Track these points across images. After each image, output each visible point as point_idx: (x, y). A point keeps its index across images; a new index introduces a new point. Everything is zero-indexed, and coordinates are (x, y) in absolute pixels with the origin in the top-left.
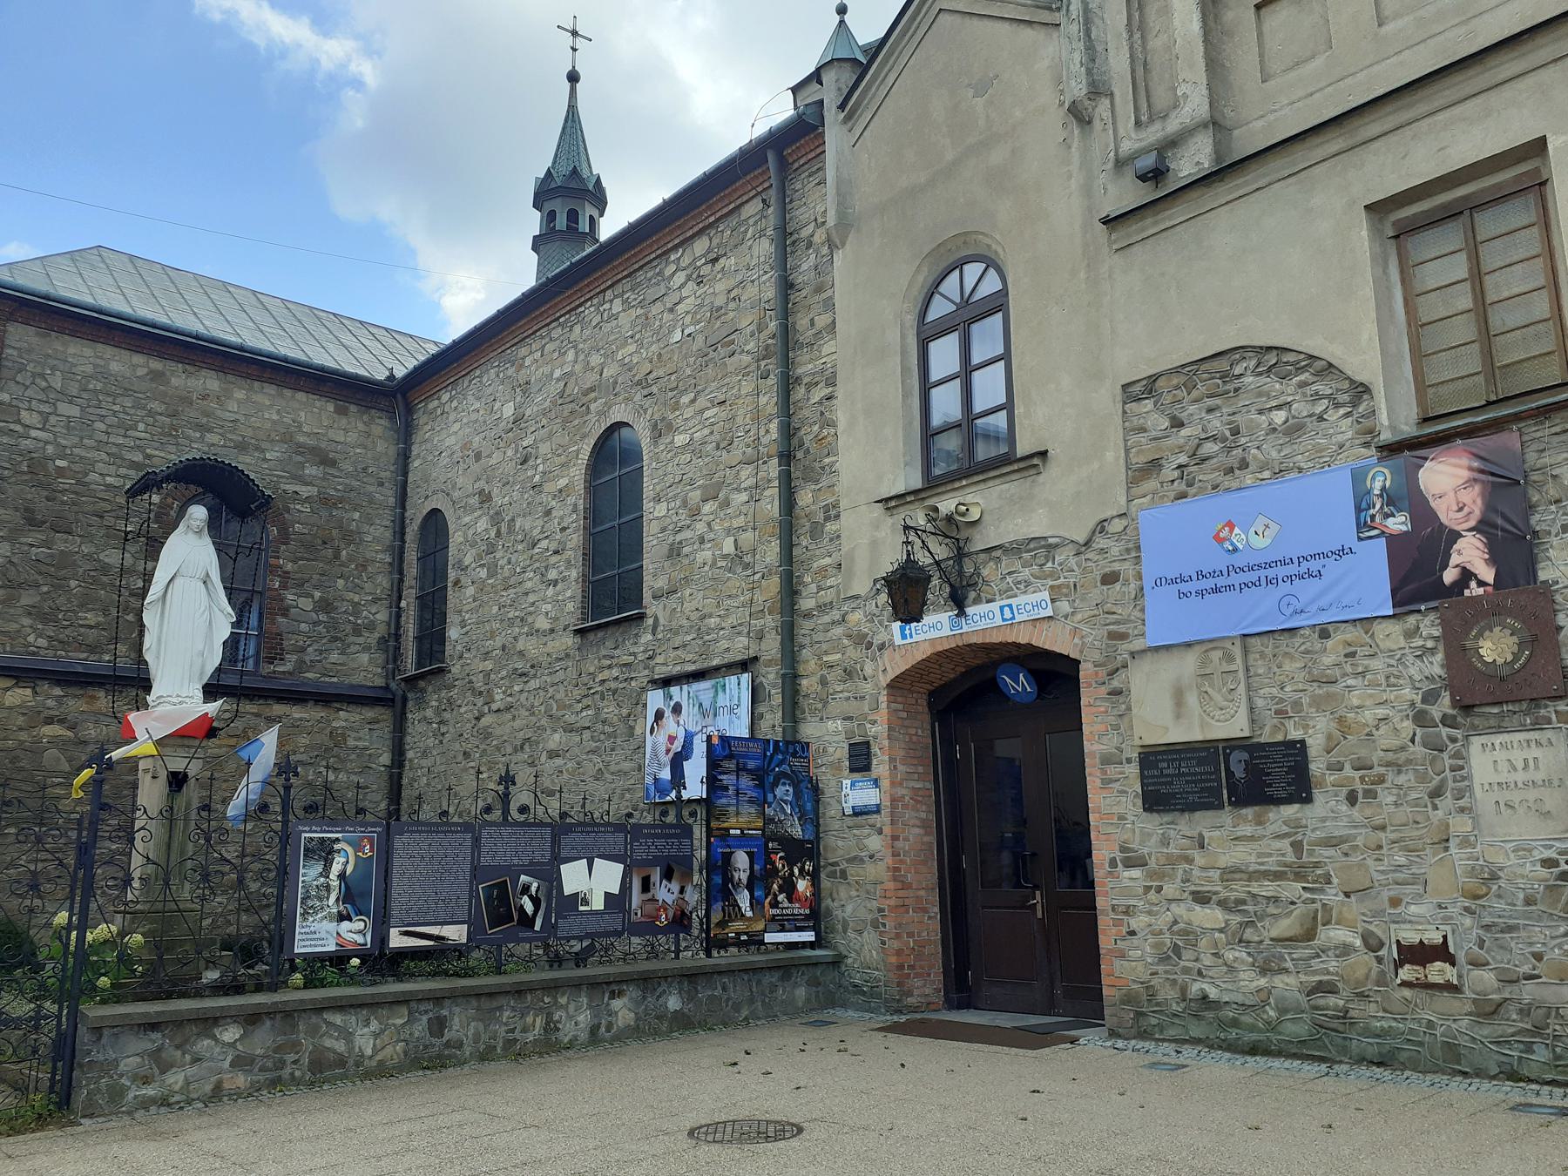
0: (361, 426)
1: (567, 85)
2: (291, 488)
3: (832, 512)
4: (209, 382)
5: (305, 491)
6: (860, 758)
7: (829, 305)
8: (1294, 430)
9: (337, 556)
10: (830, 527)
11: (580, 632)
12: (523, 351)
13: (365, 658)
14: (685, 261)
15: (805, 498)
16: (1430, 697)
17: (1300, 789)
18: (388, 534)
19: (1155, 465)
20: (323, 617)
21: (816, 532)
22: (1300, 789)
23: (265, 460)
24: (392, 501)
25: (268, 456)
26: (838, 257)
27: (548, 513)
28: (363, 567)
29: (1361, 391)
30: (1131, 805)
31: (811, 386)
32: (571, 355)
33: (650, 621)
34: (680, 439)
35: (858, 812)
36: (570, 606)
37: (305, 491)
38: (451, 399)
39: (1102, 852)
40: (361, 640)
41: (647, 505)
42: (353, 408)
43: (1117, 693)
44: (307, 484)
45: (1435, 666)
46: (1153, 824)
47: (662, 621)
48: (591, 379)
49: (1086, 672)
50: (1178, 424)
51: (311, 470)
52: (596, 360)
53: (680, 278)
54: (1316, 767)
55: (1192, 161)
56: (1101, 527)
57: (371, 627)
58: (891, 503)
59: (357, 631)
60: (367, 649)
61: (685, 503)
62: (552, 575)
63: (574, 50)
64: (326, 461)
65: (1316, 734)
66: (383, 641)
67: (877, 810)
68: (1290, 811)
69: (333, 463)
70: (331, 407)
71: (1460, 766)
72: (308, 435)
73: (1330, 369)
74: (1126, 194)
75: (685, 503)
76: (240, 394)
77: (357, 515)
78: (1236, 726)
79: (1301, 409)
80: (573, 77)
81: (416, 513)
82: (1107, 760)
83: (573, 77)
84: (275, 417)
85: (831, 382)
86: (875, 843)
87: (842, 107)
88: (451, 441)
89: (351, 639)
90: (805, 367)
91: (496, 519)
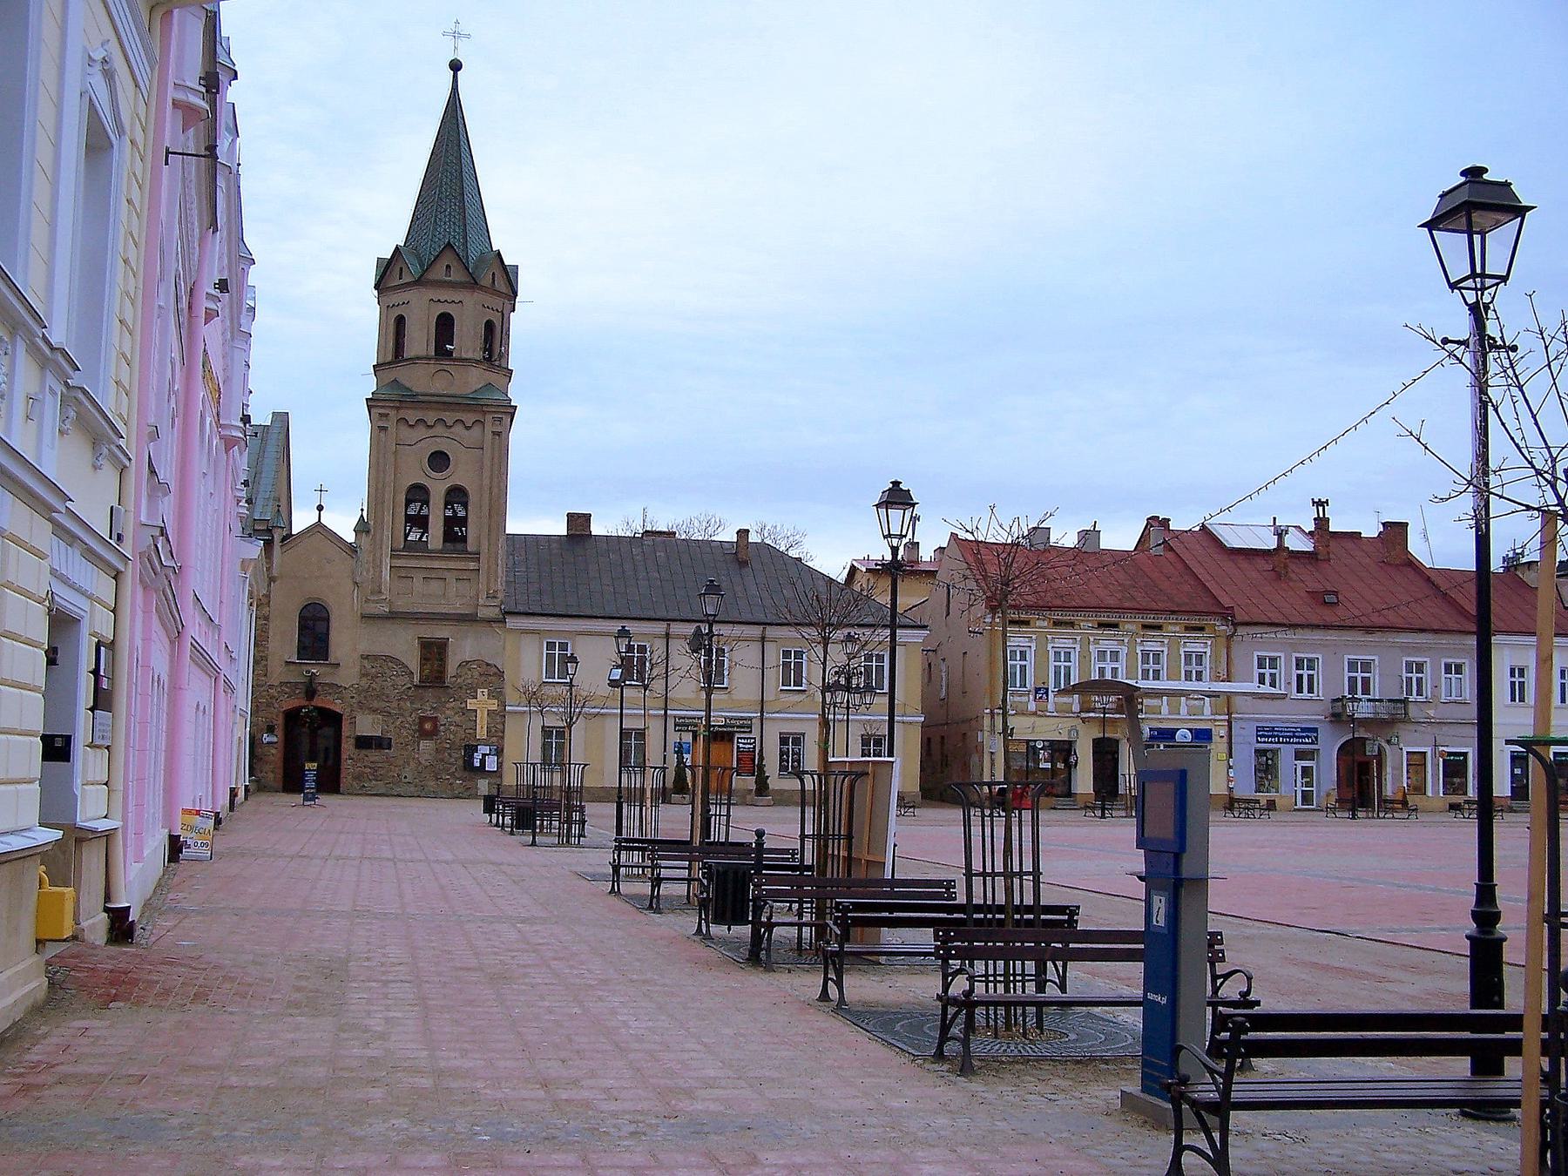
6: (271, 730)
10: (264, 663)
30: (352, 748)
35: (268, 743)
39: (344, 756)
67: (276, 743)
86: (274, 751)
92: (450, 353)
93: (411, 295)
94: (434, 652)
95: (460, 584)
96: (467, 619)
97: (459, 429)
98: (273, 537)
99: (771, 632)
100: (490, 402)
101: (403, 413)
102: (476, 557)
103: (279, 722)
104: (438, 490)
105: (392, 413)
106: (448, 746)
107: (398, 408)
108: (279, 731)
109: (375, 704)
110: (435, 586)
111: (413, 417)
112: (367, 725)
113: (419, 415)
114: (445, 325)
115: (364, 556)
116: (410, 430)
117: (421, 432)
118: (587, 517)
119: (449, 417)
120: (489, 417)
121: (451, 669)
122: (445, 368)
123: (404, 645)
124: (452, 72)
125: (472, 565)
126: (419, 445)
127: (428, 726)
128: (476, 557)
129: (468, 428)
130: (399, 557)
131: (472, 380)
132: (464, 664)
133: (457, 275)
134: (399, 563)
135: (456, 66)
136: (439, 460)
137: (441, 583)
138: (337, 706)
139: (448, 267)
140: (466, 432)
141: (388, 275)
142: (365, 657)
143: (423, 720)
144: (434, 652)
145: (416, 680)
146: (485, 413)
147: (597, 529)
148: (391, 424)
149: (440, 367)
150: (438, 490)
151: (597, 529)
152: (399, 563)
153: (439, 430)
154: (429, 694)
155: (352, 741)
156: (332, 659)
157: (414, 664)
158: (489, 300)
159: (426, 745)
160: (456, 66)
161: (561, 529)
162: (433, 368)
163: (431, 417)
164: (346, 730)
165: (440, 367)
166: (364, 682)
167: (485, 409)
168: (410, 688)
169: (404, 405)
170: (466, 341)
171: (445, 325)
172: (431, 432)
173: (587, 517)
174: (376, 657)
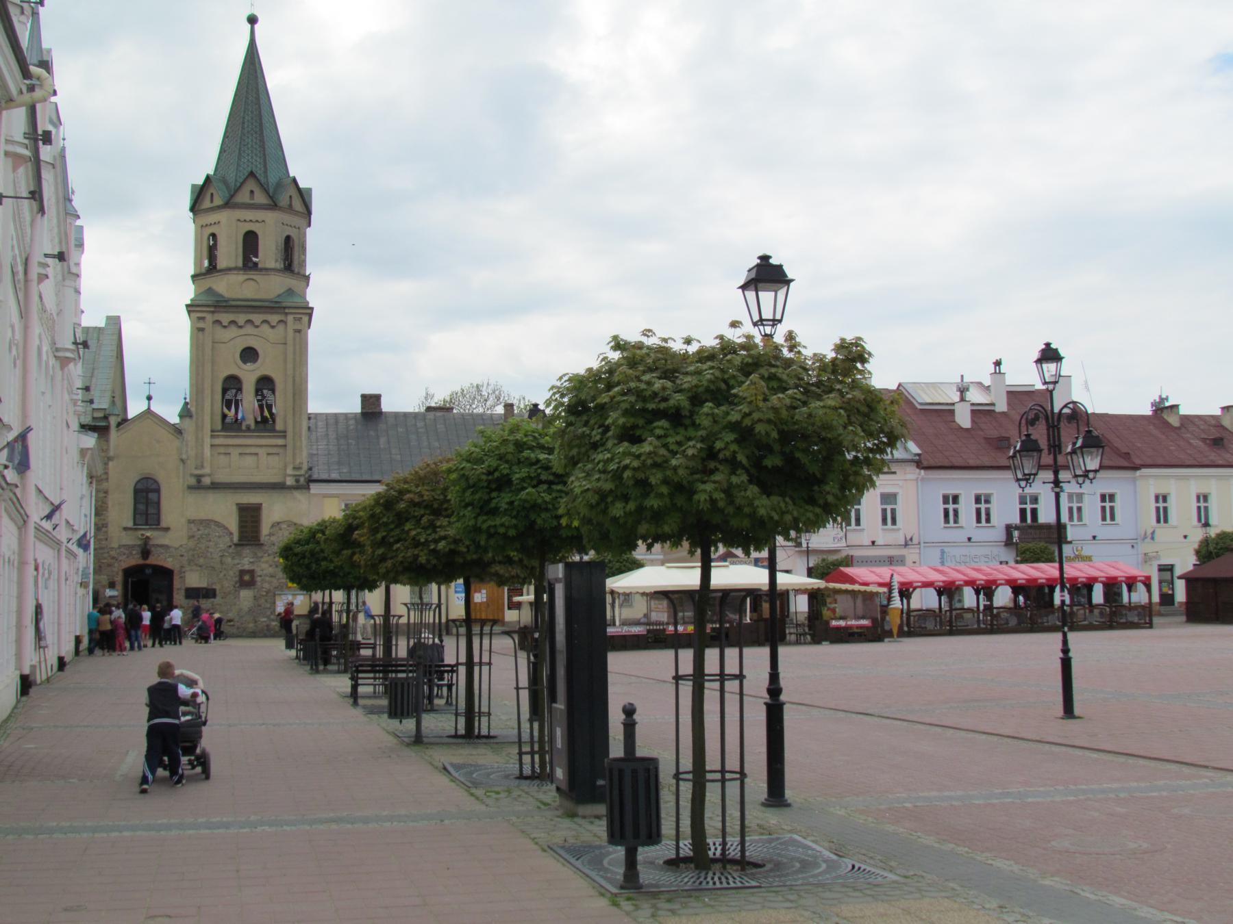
6: (112, 585)
8: (219, 537)
10: (104, 529)
16: (236, 583)
17: (214, 596)
19: (193, 536)
22: (214, 596)
29: (231, 534)
43: (181, 577)
45: (237, 579)
46: (187, 601)
49: (175, 572)
50: (199, 530)
54: (218, 592)
55: (207, 481)
56: (181, 546)
58: (126, 529)
65: (217, 587)
67: (117, 597)
68: (213, 600)
71: (239, 594)
73: (226, 528)
74: (193, 481)
78: (204, 585)
79: (221, 533)
82: (178, 589)
92: (256, 264)
93: (224, 217)
94: (250, 517)
95: (270, 458)
96: (278, 487)
97: (265, 327)
98: (109, 423)
100: (289, 305)
101: (218, 316)
102: (283, 434)
103: (119, 579)
104: (249, 375)
105: (209, 317)
106: (264, 593)
107: (213, 312)
108: (119, 586)
109: (202, 560)
110: (250, 461)
111: (225, 318)
112: (194, 580)
113: (232, 317)
114: (250, 242)
115: (189, 436)
116: (223, 330)
117: (233, 331)
118: (377, 398)
119: (257, 318)
120: (290, 318)
121: (265, 529)
122: (254, 277)
123: (224, 510)
124: (249, 26)
125: (280, 442)
127: (247, 578)
128: (283, 434)
129: (273, 327)
130: (218, 436)
131: (272, 286)
132: (277, 525)
133: (260, 198)
134: (217, 441)
135: (252, 20)
137: (254, 458)
138: (169, 563)
139: (252, 192)
140: (271, 330)
141: (200, 198)
142: (190, 522)
143: (242, 572)
144: (250, 517)
145: (236, 539)
146: (286, 314)
147: (387, 406)
148: (208, 325)
150: (249, 375)
152: (217, 441)
153: (249, 329)
154: (247, 551)
155: (183, 592)
156: (163, 524)
157: (233, 524)
158: (287, 218)
159: (246, 595)
160: (252, 20)
161: (356, 408)
162: (241, 277)
163: (241, 318)
164: (177, 583)
165: (246, 277)
166: (191, 544)
167: (287, 311)
168: (230, 546)
169: (218, 310)
170: (268, 254)
171: (250, 242)
172: (242, 331)
173: (377, 398)
174: (201, 522)
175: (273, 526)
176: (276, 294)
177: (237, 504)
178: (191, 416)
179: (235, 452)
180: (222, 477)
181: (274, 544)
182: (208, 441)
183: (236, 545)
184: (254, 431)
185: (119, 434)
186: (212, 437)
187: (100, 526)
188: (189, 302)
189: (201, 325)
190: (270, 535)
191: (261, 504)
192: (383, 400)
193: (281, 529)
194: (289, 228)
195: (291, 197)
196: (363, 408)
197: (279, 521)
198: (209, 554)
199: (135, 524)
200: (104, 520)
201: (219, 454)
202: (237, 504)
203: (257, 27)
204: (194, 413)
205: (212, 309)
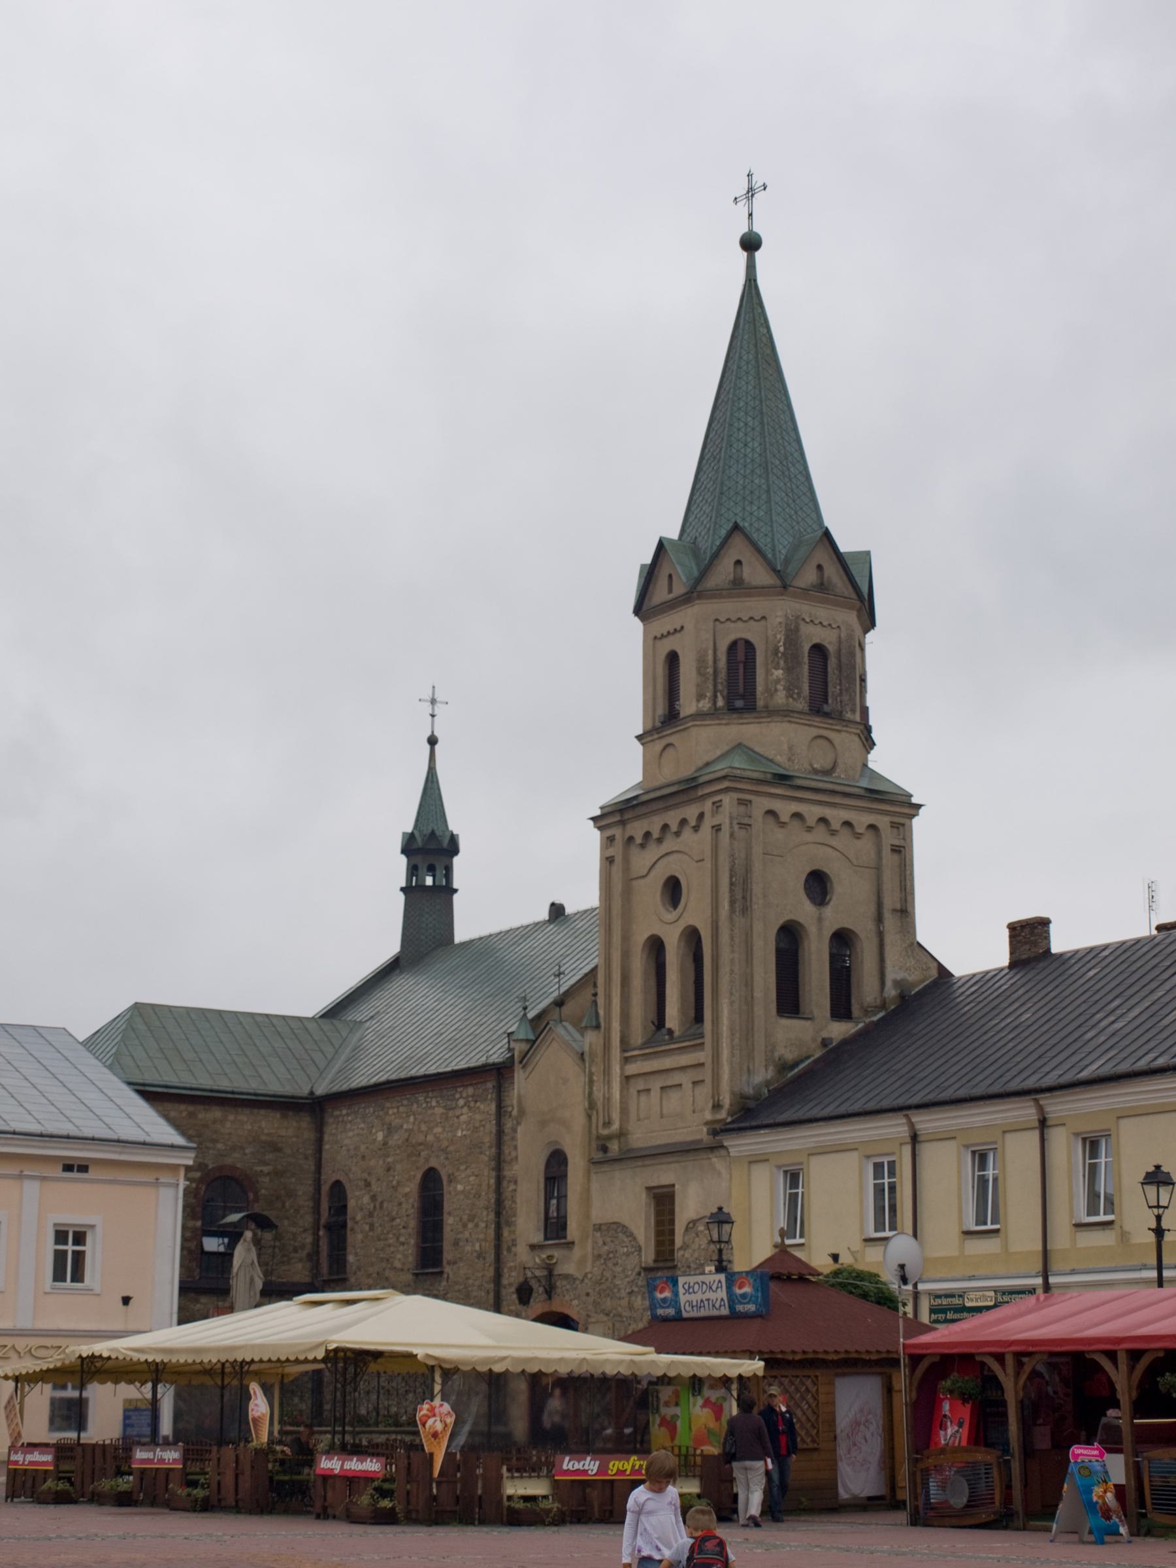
0: (295, 1124)
1: (428, 747)
2: (259, 1168)
3: (514, 1243)
4: (216, 1113)
5: (266, 1169)
7: (516, 1148)
9: (283, 1206)
11: (416, 1275)
12: (388, 1105)
13: (300, 1266)
14: (464, 1095)
15: (506, 1232)
18: (311, 1189)
19: (599, 1256)
20: (277, 1244)
21: (509, 1250)
23: (245, 1154)
24: (313, 1168)
25: (247, 1151)
26: (519, 1129)
27: (400, 1204)
28: (297, 1211)
31: (509, 1182)
32: (412, 1119)
33: (445, 1276)
34: (460, 1187)
36: (411, 1259)
37: (266, 1169)
38: (348, 1115)
40: (297, 1255)
41: (445, 1216)
42: (291, 1113)
44: (266, 1164)
47: (451, 1276)
48: (421, 1138)
51: (269, 1156)
52: (424, 1127)
53: (461, 1102)
57: (303, 1247)
58: (533, 1247)
59: (295, 1250)
60: (301, 1260)
61: (461, 1220)
62: (402, 1239)
63: (433, 716)
64: (276, 1148)
66: (309, 1255)
69: (279, 1150)
70: (278, 1115)
72: (268, 1135)
75: (461, 1220)
76: (231, 1117)
77: (293, 1180)
80: (432, 741)
81: (329, 1177)
83: (432, 741)
84: (250, 1127)
85: (516, 1182)
87: (521, 1062)
88: (347, 1141)
89: (292, 1255)
90: (507, 1173)
91: (373, 1198)
97: (687, 833)
99: (1057, 1107)
107: (623, 823)
111: (637, 829)
124: (744, 255)
126: (652, 874)
132: (692, 1224)
134: (632, 1069)
135: (751, 244)
136: (673, 890)
146: (704, 797)
147: (1060, 942)
148: (617, 850)
149: (664, 742)
151: (1060, 942)
152: (632, 1069)
153: (669, 844)
160: (751, 244)
167: (700, 793)
169: (626, 816)
175: (687, 1229)
176: (700, 763)
177: (649, 1189)
178: (598, 1027)
179: (656, 1084)
180: (639, 1138)
181: (689, 1267)
182: (616, 1069)
183: (647, 1270)
184: (682, 1038)
185: (529, 1069)
186: (626, 1060)
187: (510, 1243)
188: (598, 812)
189: (610, 852)
190: (685, 1247)
191: (673, 1186)
192: (1053, 929)
193: (697, 1235)
194: (740, 624)
195: (738, 563)
196: (1013, 951)
197: (695, 1218)
198: (616, 1290)
199: (546, 1238)
200: (514, 1232)
201: (639, 1092)
202: (649, 1189)
203: (758, 255)
204: (602, 1024)
205: (617, 818)
